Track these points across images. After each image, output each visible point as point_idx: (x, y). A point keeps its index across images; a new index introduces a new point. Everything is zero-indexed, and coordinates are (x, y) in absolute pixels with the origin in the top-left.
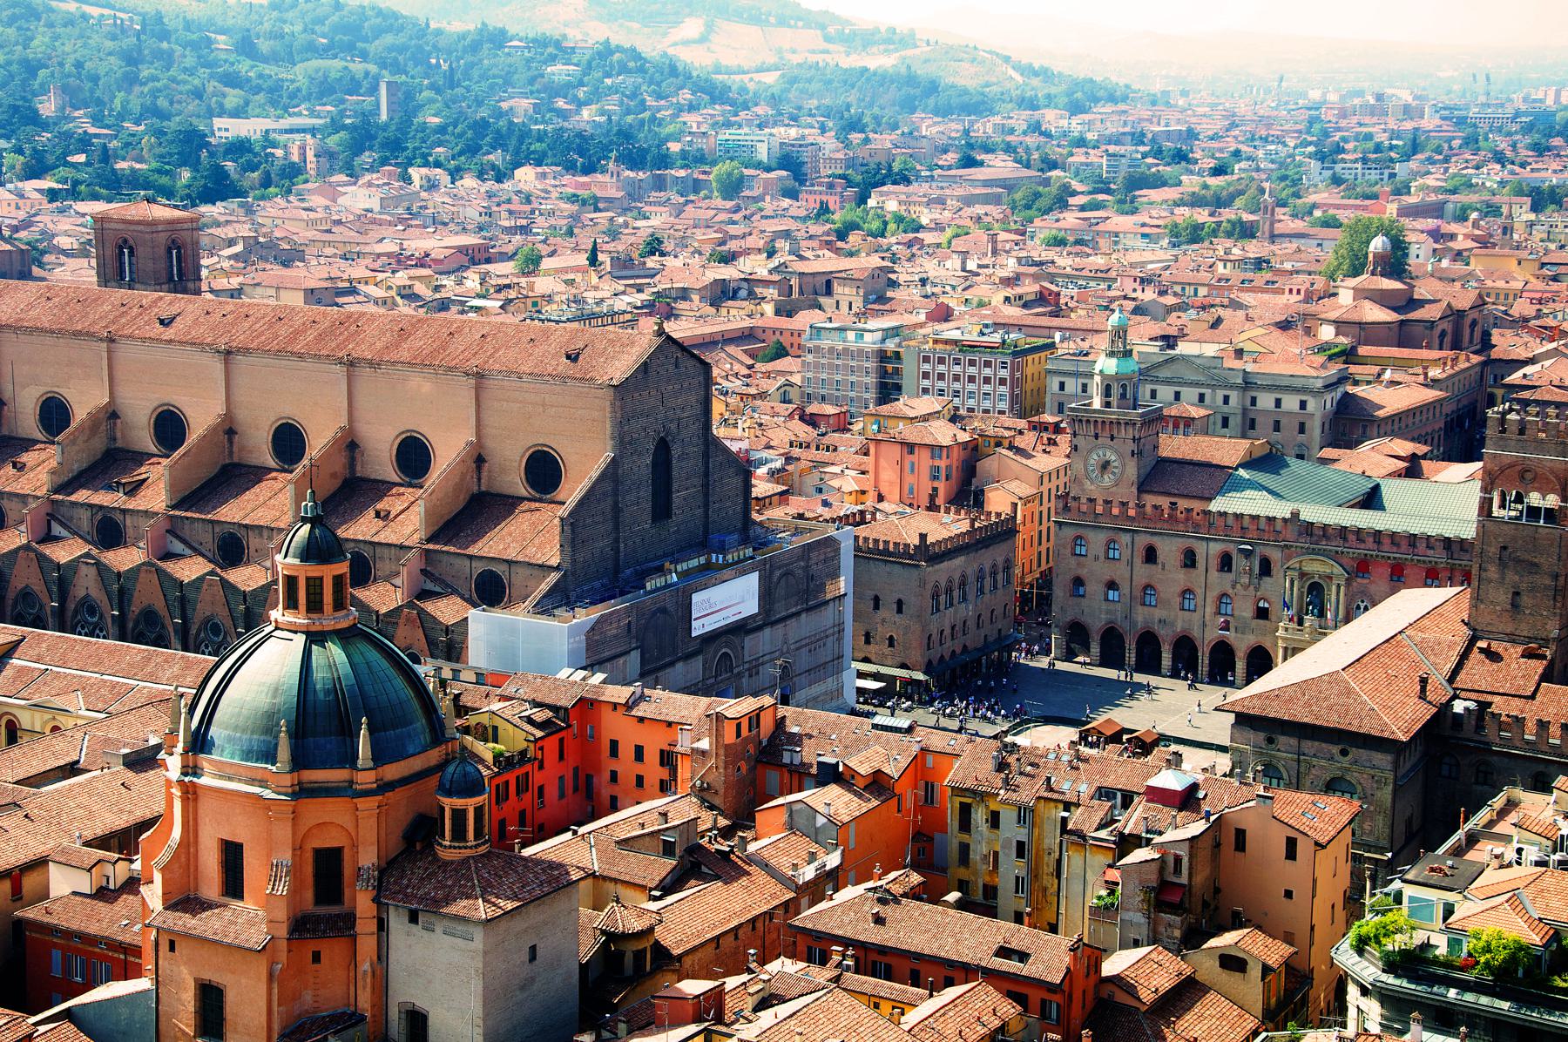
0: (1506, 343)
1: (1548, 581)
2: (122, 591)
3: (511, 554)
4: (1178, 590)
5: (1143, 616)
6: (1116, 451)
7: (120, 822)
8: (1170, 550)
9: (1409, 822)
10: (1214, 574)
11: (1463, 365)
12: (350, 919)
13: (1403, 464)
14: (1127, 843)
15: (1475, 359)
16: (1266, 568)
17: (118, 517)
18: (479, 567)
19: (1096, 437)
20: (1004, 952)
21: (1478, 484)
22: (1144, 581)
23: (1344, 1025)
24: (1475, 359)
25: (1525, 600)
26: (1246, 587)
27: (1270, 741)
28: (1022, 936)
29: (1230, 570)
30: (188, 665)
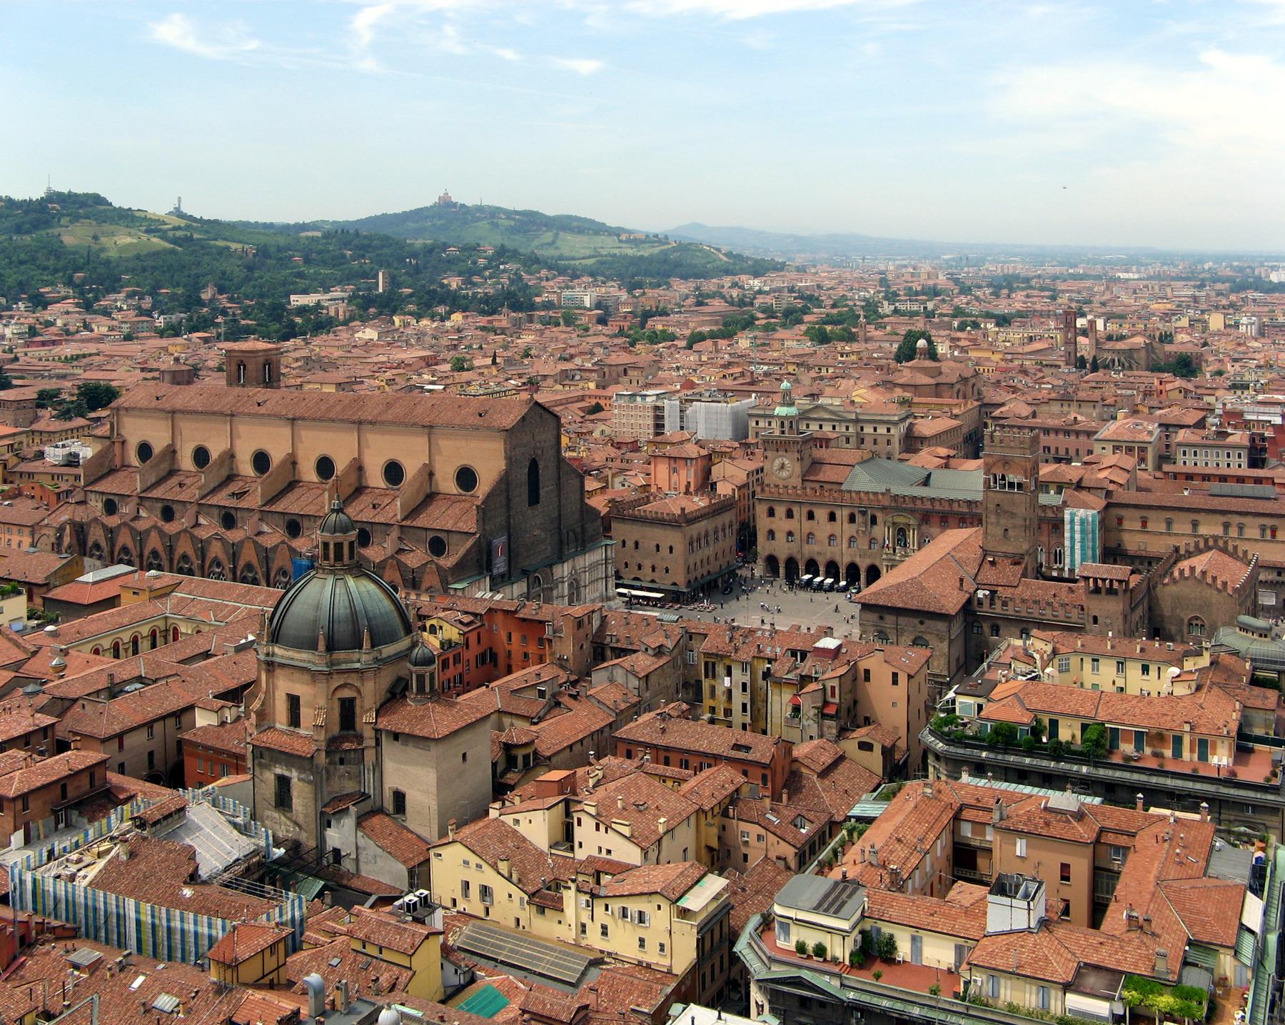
0: (992, 395)
1: (1021, 522)
2: (234, 554)
3: (449, 526)
7: (233, 684)
8: (821, 514)
9: (958, 660)
10: (846, 525)
11: (969, 406)
12: (360, 738)
13: (943, 461)
14: (805, 680)
15: (976, 403)
16: (874, 521)
17: (233, 512)
18: (431, 535)
20: (737, 747)
21: (982, 472)
22: (808, 531)
23: (927, 777)
24: (976, 403)
25: (1010, 533)
27: (881, 618)
28: (747, 738)
30: (270, 595)
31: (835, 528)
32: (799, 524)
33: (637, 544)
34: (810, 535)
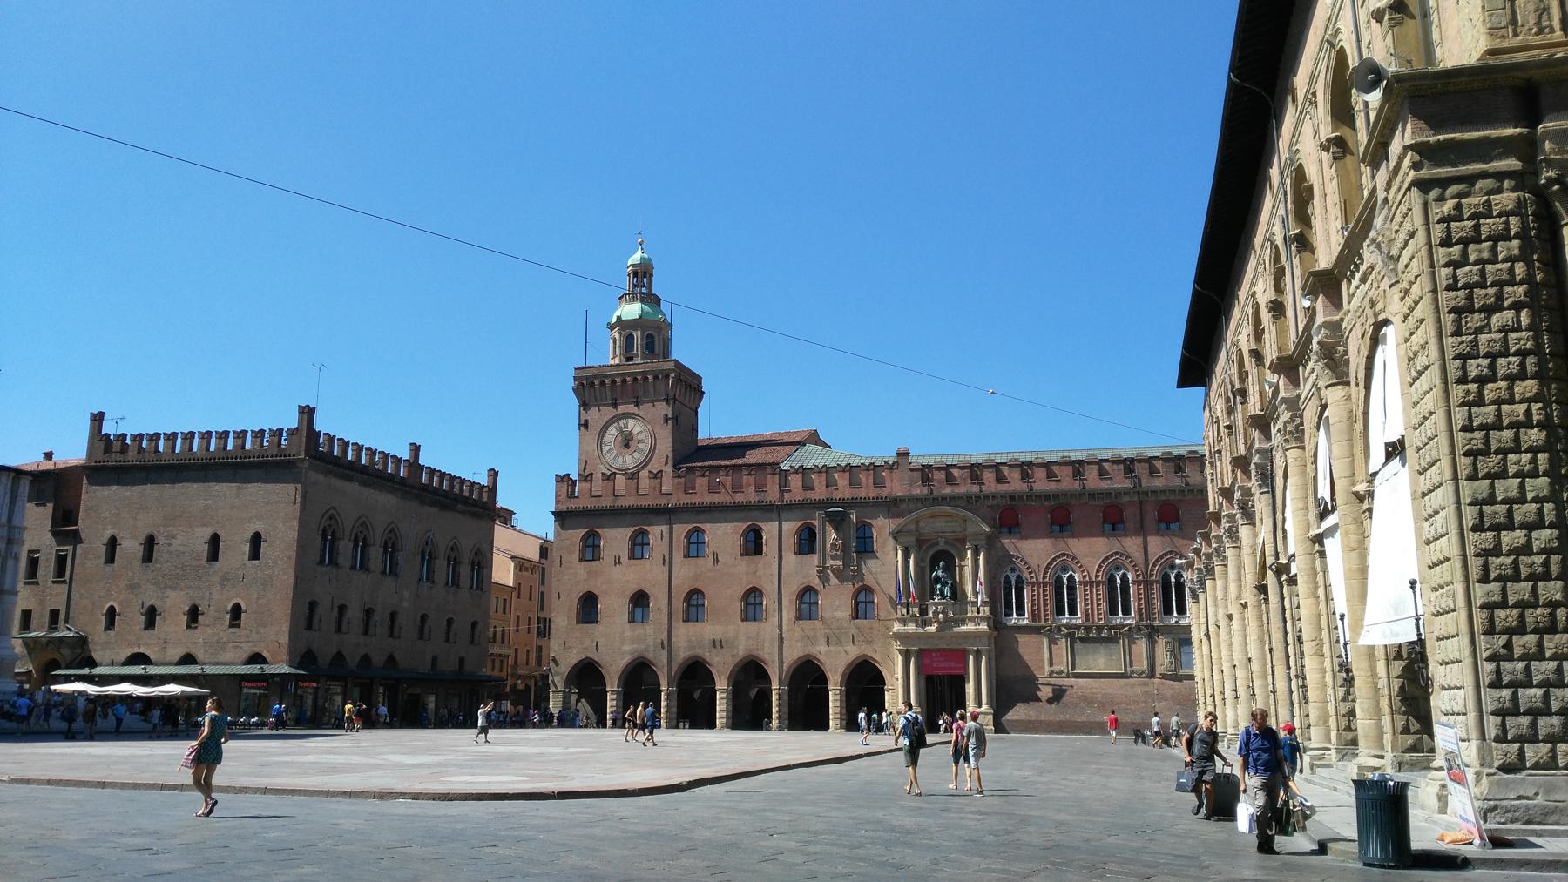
4: (741, 592)
5: (689, 639)
10: (790, 559)
19: (615, 406)
29: (812, 551)
31: (764, 571)
33: (150, 542)
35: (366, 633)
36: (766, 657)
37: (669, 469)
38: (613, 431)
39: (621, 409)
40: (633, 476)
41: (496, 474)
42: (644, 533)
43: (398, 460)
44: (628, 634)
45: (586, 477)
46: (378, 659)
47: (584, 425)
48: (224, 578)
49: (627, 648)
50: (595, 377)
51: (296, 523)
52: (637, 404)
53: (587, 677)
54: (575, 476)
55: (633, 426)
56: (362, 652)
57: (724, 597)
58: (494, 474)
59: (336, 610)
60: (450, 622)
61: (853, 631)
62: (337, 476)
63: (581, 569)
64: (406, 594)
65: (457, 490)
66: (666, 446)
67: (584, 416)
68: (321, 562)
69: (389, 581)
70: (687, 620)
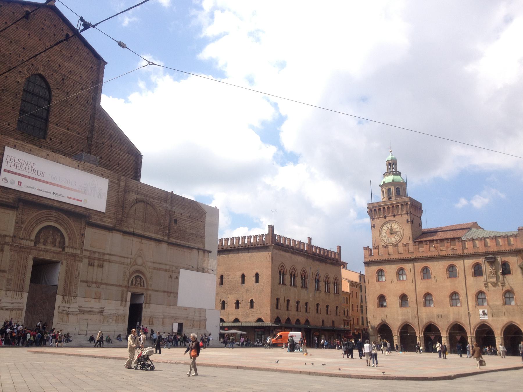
4: (448, 293)
5: (427, 314)
6: (397, 222)
10: (471, 279)
19: (385, 217)
22: (424, 292)
26: (495, 285)
31: (458, 285)
32: (411, 283)
34: (428, 297)
35: (297, 310)
36: (464, 322)
37: (411, 242)
38: (385, 228)
39: (388, 219)
40: (396, 246)
41: (340, 247)
42: (402, 269)
43: (304, 244)
44: (400, 312)
45: (376, 247)
46: (303, 321)
47: (373, 226)
48: (247, 290)
49: (400, 318)
50: (376, 207)
51: (270, 269)
52: (394, 216)
53: (384, 330)
54: (371, 247)
55: (395, 226)
56: (297, 318)
57: (441, 295)
58: (339, 248)
59: (286, 302)
60: (327, 306)
61: (504, 310)
62: (283, 251)
63: (377, 285)
64: (311, 296)
65: (326, 253)
66: (408, 232)
67: (373, 222)
68: (280, 283)
69: (304, 291)
70: (425, 306)
